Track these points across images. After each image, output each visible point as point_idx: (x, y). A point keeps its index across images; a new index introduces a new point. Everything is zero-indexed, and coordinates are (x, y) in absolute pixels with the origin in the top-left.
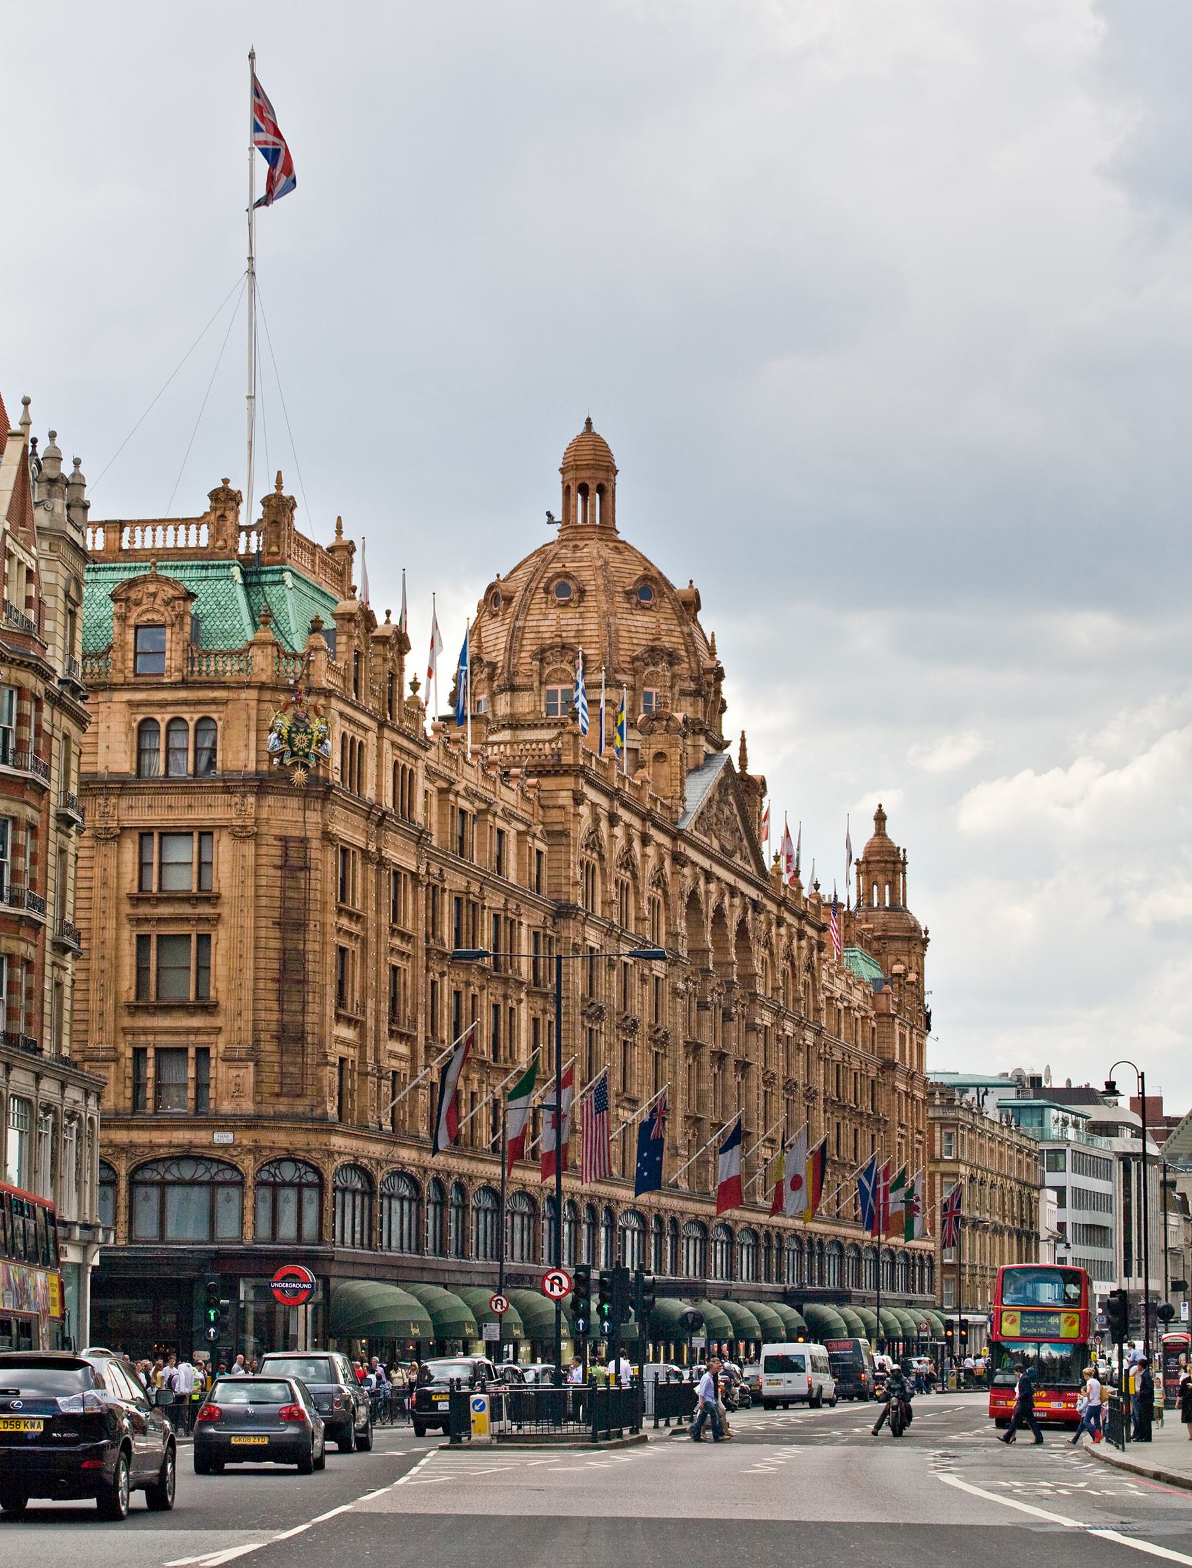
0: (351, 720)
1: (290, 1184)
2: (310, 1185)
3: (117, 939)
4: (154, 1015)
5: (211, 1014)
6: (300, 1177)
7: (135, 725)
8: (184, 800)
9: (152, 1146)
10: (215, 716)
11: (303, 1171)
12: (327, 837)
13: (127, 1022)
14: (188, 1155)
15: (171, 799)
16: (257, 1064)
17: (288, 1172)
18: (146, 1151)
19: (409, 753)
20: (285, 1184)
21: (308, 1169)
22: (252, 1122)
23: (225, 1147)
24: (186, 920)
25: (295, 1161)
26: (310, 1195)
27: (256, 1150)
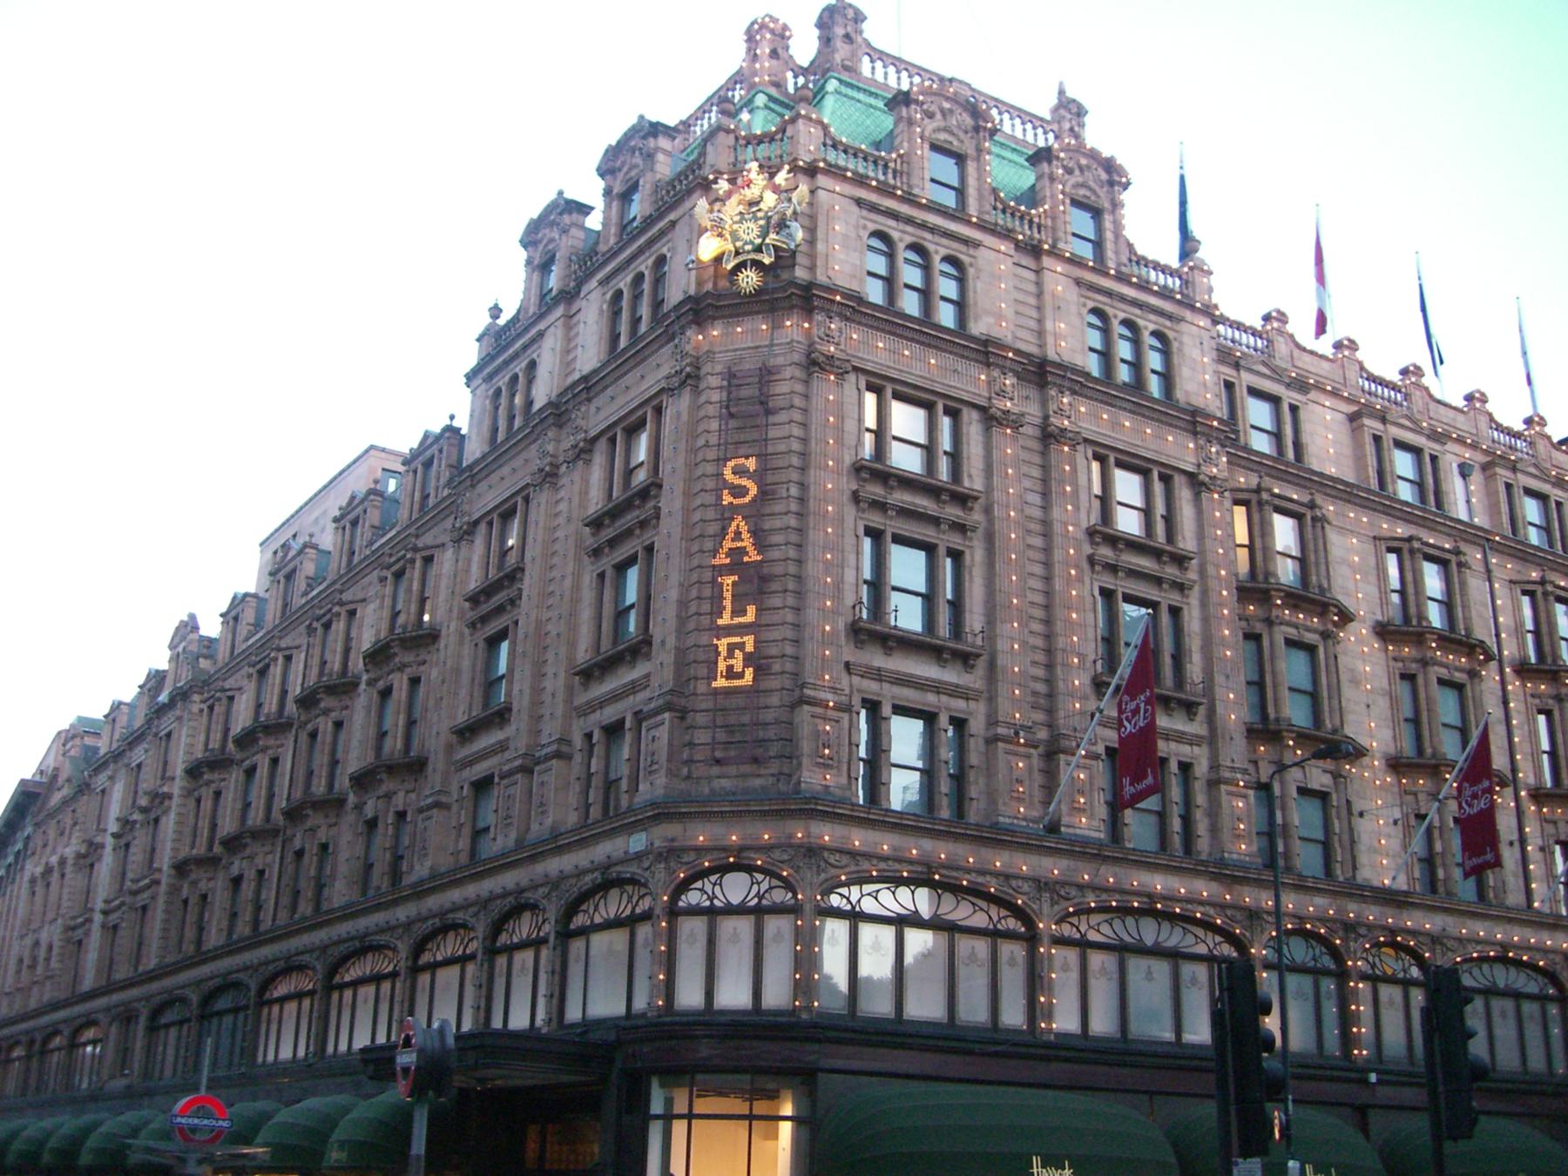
0: (873, 208)
3: (576, 587)
4: (601, 679)
5: (648, 656)
6: (760, 896)
7: (605, 307)
8: (637, 373)
9: (580, 873)
10: (665, 250)
11: (765, 886)
12: (814, 364)
13: (581, 699)
14: (609, 881)
15: (629, 379)
16: (683, 714)
17: (736, 888)
18: (573, 881)
19: (1170, 317)
20: (731, 910)
21: (775, 882)
22: (662, 813)
23: (639, 856)
24: (628, 533)
25: (750, 869)
27: (671, 853)
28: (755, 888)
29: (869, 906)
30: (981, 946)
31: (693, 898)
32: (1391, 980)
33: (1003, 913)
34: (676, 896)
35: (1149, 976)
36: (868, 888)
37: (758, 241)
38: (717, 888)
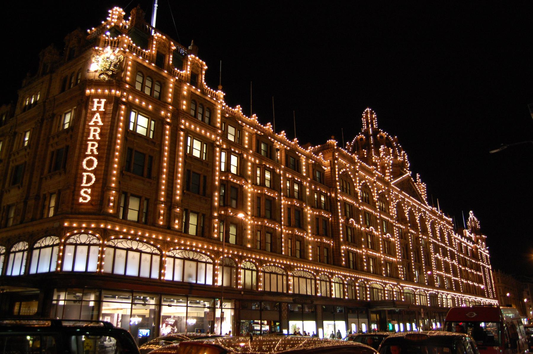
1: (84, 244)
2: (94, 245)
11: (91, 239)
17: (83, 239)
20: (81, 244)
21: (94, 237)
25: (88, 234)
26: (94, 250)
28: (89, 239)
29: (119, 245)
30: (149, 256)
31: (71, 241)
32: (249, 269)
33: (155, 248)
34: (65, 241)
35: (190, 266)
36: (119, 240)
37: (108, 68)
38: (78, 238)
